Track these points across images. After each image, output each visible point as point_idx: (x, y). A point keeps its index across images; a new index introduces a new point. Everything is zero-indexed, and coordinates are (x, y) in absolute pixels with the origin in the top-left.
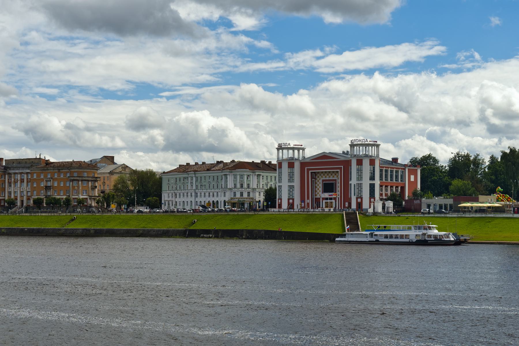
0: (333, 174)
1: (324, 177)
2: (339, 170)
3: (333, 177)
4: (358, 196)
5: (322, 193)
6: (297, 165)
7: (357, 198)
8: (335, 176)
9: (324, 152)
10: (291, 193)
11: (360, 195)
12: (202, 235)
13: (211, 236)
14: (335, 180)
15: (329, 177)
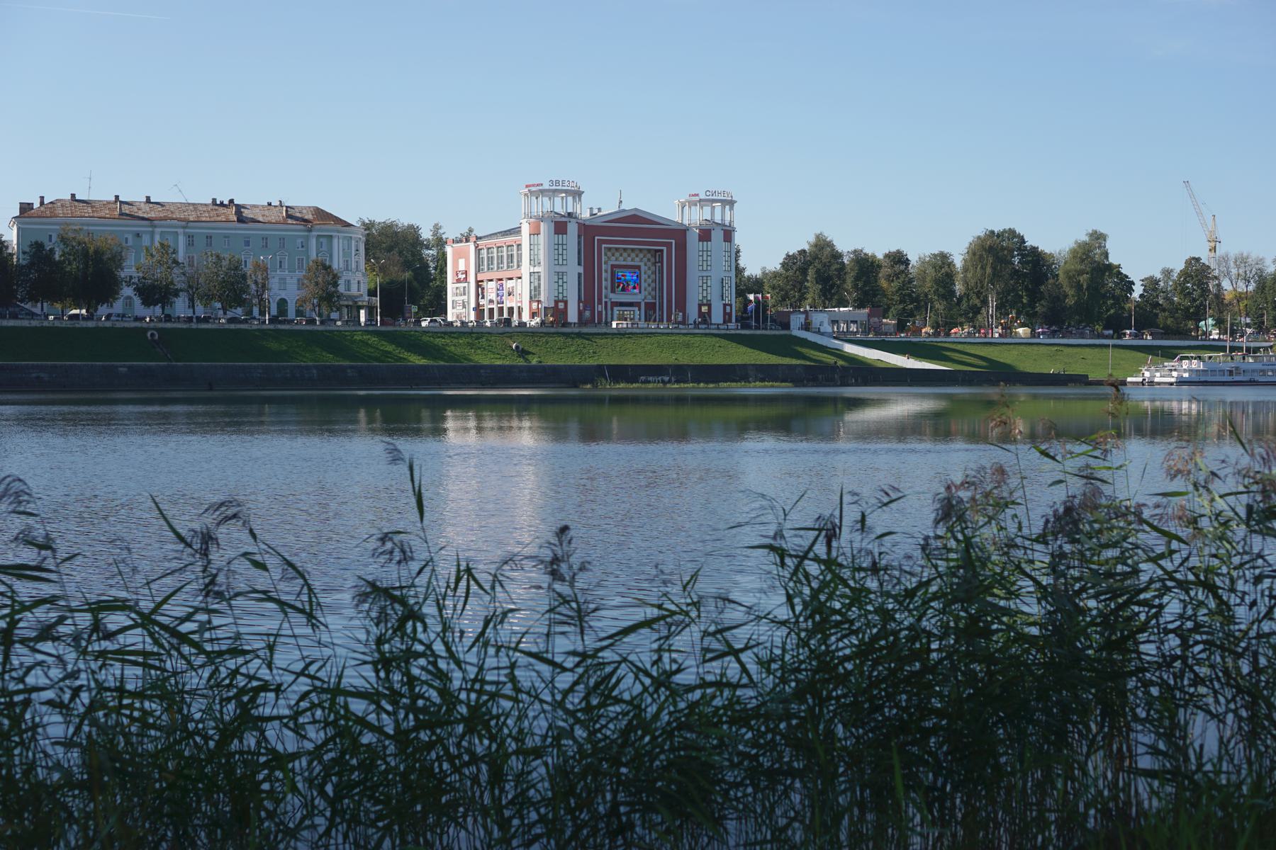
0: (633, 255)
1: (613, 258)
2: (665, 249)
3: (632, 260)
4: (561, 296)
5: (613, 291)
6: (572, 229)
7: (725, 305)
8: (637, 259)
9: (636, 209)
10: (561, 288)
11: (561, 296)
12: (643, 378)
13: (666, 379)
14: (639, 267)
15: (632, 260)
